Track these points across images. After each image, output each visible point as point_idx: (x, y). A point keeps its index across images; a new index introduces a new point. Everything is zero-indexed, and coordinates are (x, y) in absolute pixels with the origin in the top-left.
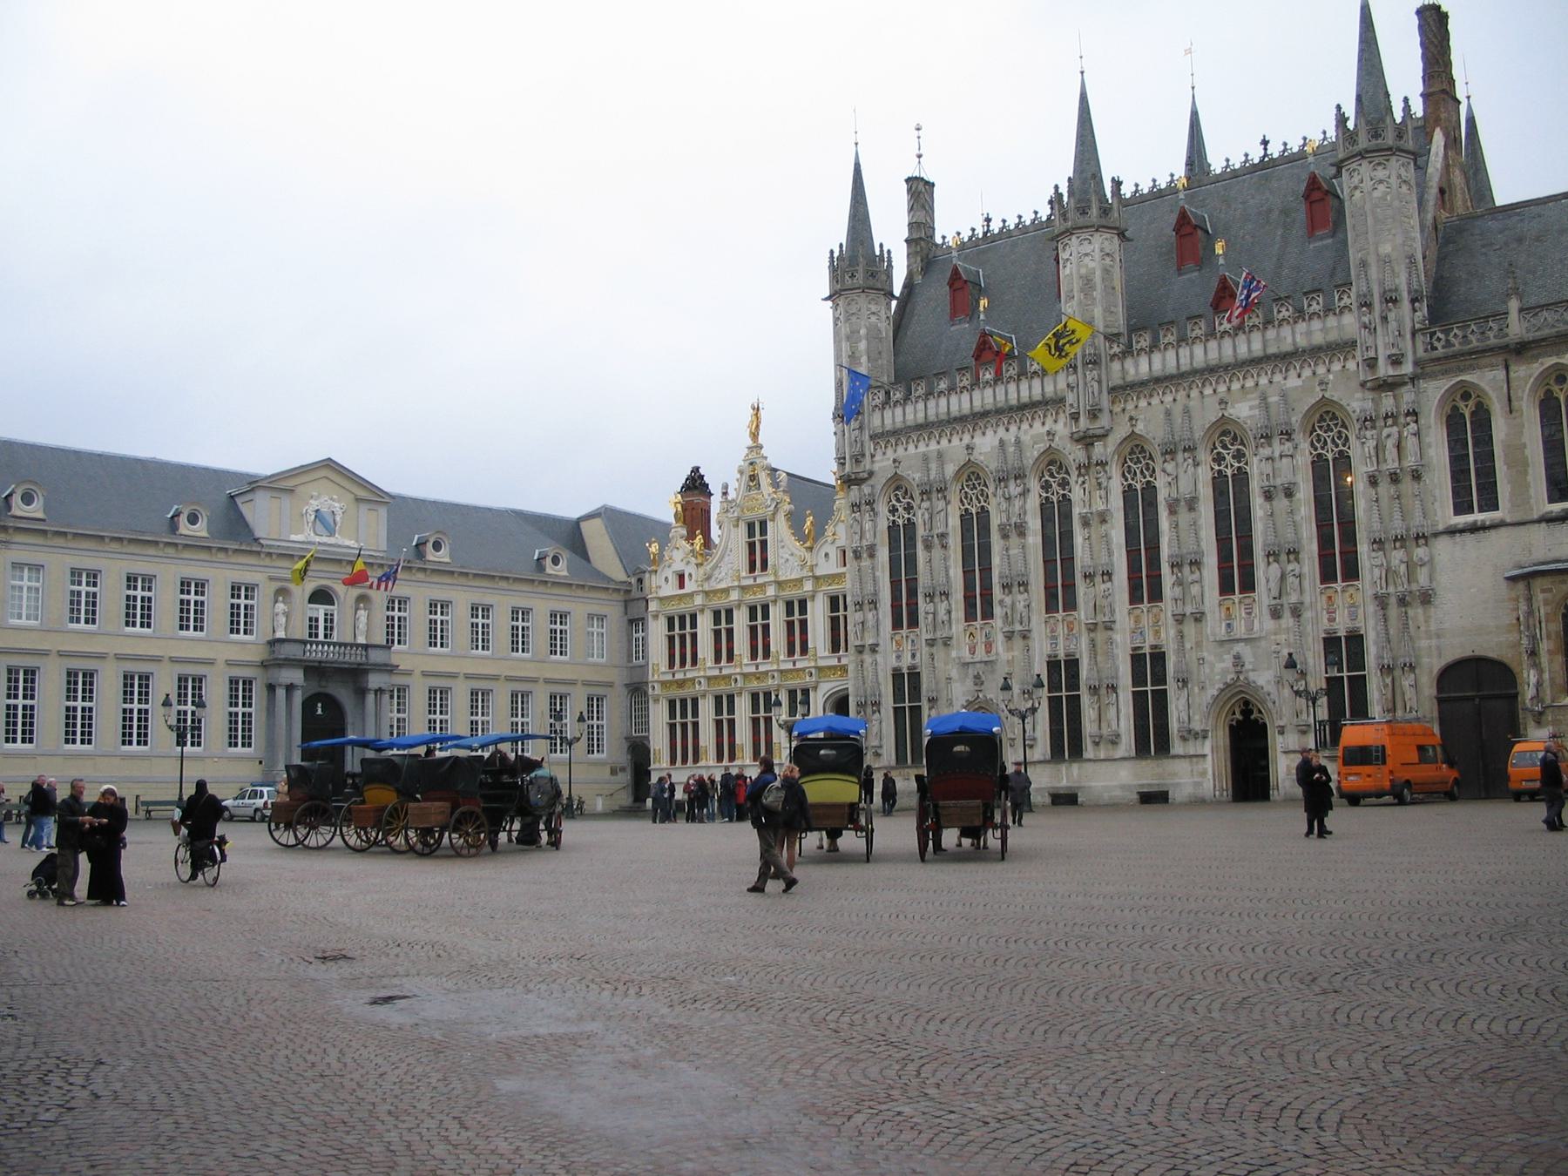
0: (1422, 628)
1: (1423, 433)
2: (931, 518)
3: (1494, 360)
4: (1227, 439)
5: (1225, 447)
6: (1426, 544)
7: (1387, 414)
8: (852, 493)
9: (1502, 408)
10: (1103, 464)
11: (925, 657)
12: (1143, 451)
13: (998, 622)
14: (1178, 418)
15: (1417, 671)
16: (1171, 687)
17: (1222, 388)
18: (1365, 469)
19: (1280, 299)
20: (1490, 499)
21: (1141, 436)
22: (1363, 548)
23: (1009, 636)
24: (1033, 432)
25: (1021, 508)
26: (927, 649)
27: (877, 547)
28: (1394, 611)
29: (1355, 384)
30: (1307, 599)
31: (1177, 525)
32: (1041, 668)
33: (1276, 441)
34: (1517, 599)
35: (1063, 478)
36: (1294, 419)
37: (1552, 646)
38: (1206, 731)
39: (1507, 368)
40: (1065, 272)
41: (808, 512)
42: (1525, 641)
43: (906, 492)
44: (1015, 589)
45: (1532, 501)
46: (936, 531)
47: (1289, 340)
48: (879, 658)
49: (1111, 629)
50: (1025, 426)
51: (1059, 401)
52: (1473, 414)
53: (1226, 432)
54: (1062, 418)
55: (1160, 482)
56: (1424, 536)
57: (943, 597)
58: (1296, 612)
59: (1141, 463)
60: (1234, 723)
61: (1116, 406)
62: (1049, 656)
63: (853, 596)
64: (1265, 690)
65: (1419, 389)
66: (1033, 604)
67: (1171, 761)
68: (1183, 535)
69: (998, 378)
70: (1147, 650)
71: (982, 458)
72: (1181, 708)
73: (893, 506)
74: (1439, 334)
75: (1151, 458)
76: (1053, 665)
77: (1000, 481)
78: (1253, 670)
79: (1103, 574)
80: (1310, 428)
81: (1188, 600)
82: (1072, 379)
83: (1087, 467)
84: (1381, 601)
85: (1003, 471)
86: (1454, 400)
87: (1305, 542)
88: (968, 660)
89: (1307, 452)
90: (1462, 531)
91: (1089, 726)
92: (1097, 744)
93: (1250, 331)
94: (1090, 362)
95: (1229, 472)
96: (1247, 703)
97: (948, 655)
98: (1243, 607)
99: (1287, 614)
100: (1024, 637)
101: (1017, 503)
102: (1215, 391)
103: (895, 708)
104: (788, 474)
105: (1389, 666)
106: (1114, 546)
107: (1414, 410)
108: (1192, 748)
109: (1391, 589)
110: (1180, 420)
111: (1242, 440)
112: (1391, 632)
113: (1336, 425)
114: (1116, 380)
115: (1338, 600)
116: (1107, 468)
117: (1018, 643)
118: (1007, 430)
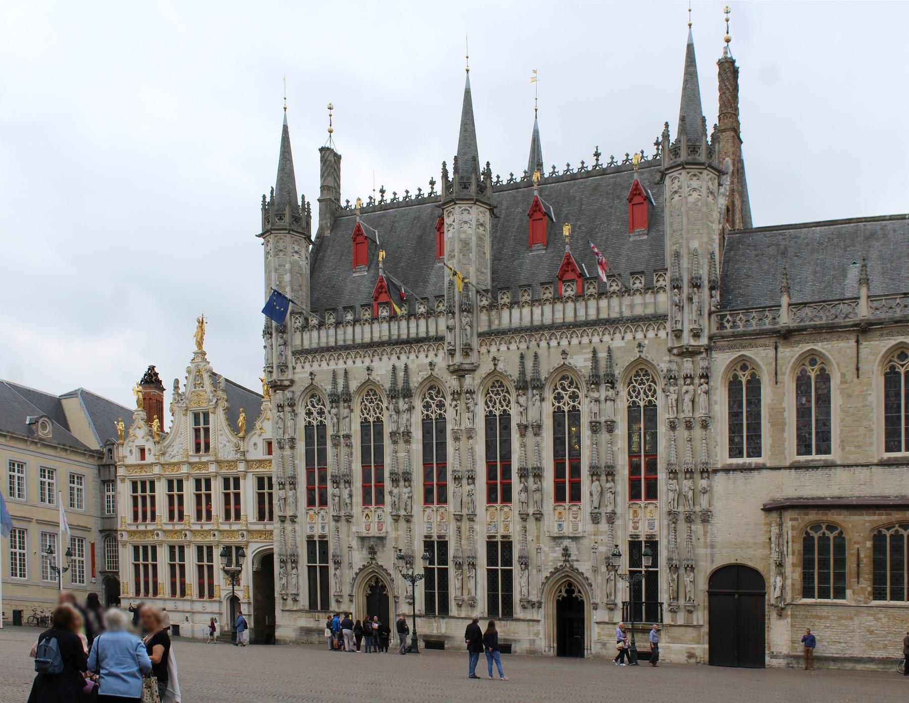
0: (702, 540)
1: (712, 392)
2: (338, 422)
3: (767, 341)
4: (566, 383)
5: (564, 389)
6: (708, 478)
7: (687, 375)
8: (277, 396)
9: (770, 379)
10: (471, 392)
11: (333, 529)
12: (502, 385)
13: (388, 508)
14: (529, 364)
15: (695, 571)
16: (516, 568)
17: (564, 342)
18: (667, 416)
19: (613, 276)
20: (755, 448)
21: (501, 373)
22: (662, 475)
23: (396, 519)
24: (418, 362)
25: (407, 420)
26: (334, 523)
27: (297, 441)
28: (682, 526)
29: (665, 350)
30: (619, 511)
31: (525, 446)
32: (419, 549)
33: (603, 387)
34: (770, 524)
35: (440, 401)
36: (616, 372)
37: (795, 561)
38: (540, 603)
40: (448, 235)
41: (241, 409)
42: (774, 556)
43: (319, 400)
44: (402, 483)
45: (787, 452)
46: (341, 433)
47: (617, 309)
48: (297, 527)
49: (474, 521)
50: (413, 356)
51: (440, 339)
52: (748, 382)
53: (565, 374)
54: (441, 353)
55: (514, 411)
56: (707, 471)
57: (347, 485)
58: (611, 518)
59: (500, 395)
60: (560, 598)
61: (482, 348)
62: (426, 537)
63: (278, 478)
64: (585, 576)
65: (711, 358)
66: (415, 497)
67: (514, 623)
68: (530, 454)
69: (393, 317)
70: (499, 539)
71: (378, 378)
72: (523, 584)
73: (309, 410)
74: (728, 317)
75: (508, 392)
77: (392, 398)
78: (577, 561)
79: (468, 478)
80: (628, 381)
81: (531, 504)
82: (451, 322)
83: (459, 394)
84: (673, 515)
85: (395, 390)
86: (735, 370)
87: (619, 467)
88: (364, 535)
89: (625, 400)
90: (734, 470)
91: (453, 592)
92: (459, 606)
93: (589, 299)
94: (466, 310)
95: (566, 409)
96: (570, 584)
97: (349, 529)
98: (571, 513)
99: (604, 520)
100: (408, 521)
101: (405, 416)
102: (559, 343)
103: (309, 567)
104: (227, 380)
105: (676, 565)
106: (477, 458)
107: (707, 374)
108: (530, 614)
109: (681, 509)
110: (531, 365)
111: (577, 384)
112: (678, 540)
113: (647, 380)
114: (484, 328)
115: (641, 513)
116: (474, 396)
117: (402, 524)
118: (399, 358)
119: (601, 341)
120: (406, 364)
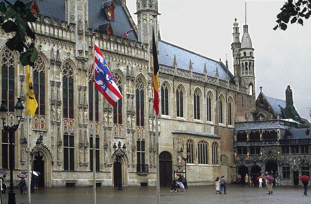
23: (52, 123)
39: (174, 81)
58: (133, 133)
71: (44, 53)
76: (66, 137)
99: (131, 132)
117: (56, 127)
119: (129, 63)
120: (58, 50)
